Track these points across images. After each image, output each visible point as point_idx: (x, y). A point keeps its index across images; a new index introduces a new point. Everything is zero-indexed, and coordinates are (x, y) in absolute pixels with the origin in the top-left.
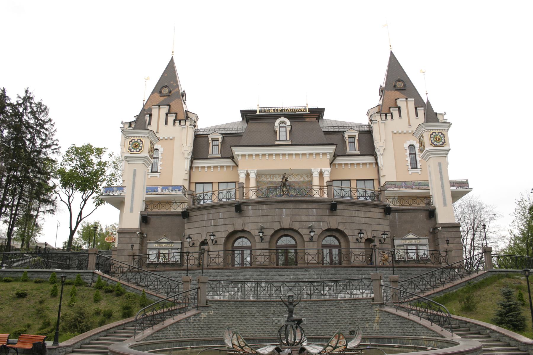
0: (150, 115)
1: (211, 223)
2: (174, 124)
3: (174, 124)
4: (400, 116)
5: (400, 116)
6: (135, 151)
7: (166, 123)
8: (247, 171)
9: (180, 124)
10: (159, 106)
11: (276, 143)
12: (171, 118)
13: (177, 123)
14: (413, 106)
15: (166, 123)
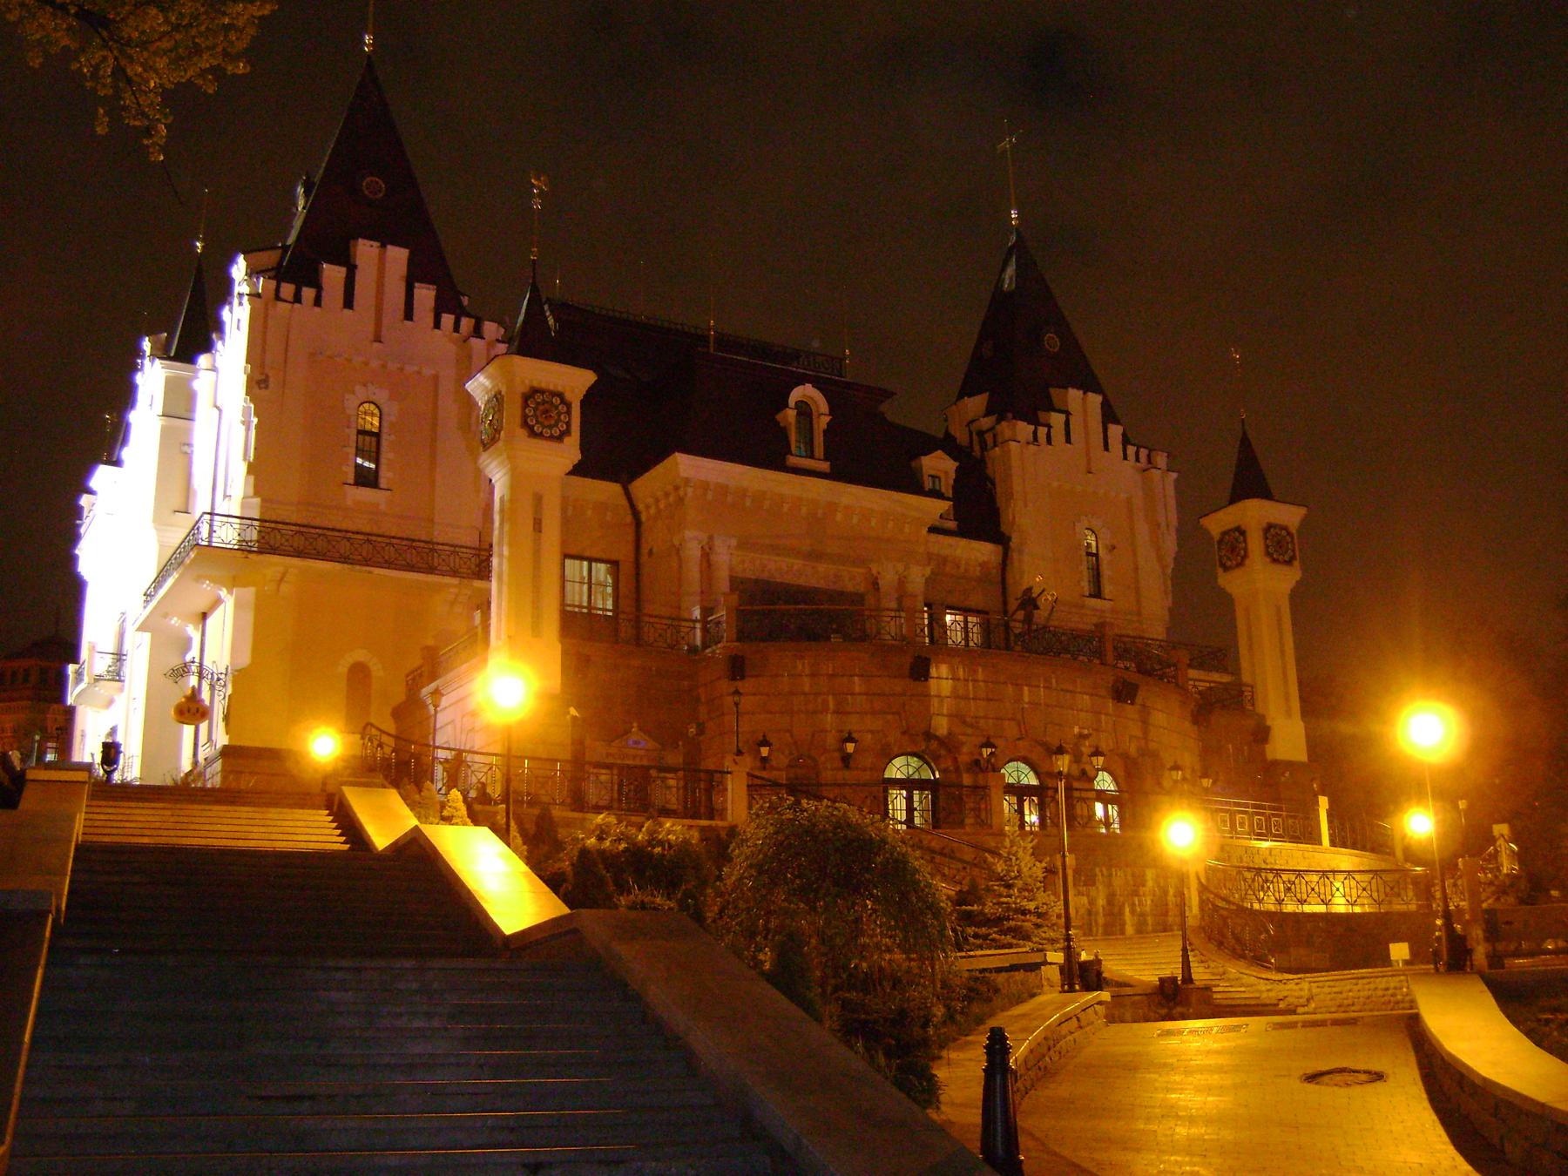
0: (352, 269)
1: (825, 702)
2: (437, 325)
3: (437, 325)
4: (1068, 440)
5: (1068, 440)
6: (547, 432)
7: (409, 314)
8: (711, 538)
9: (456, 329)
10: (383, 246)
11: (792, 460)
12: (425, 295)
13: (448, 320)
14: (1099, 418)
15: (409, 314)
